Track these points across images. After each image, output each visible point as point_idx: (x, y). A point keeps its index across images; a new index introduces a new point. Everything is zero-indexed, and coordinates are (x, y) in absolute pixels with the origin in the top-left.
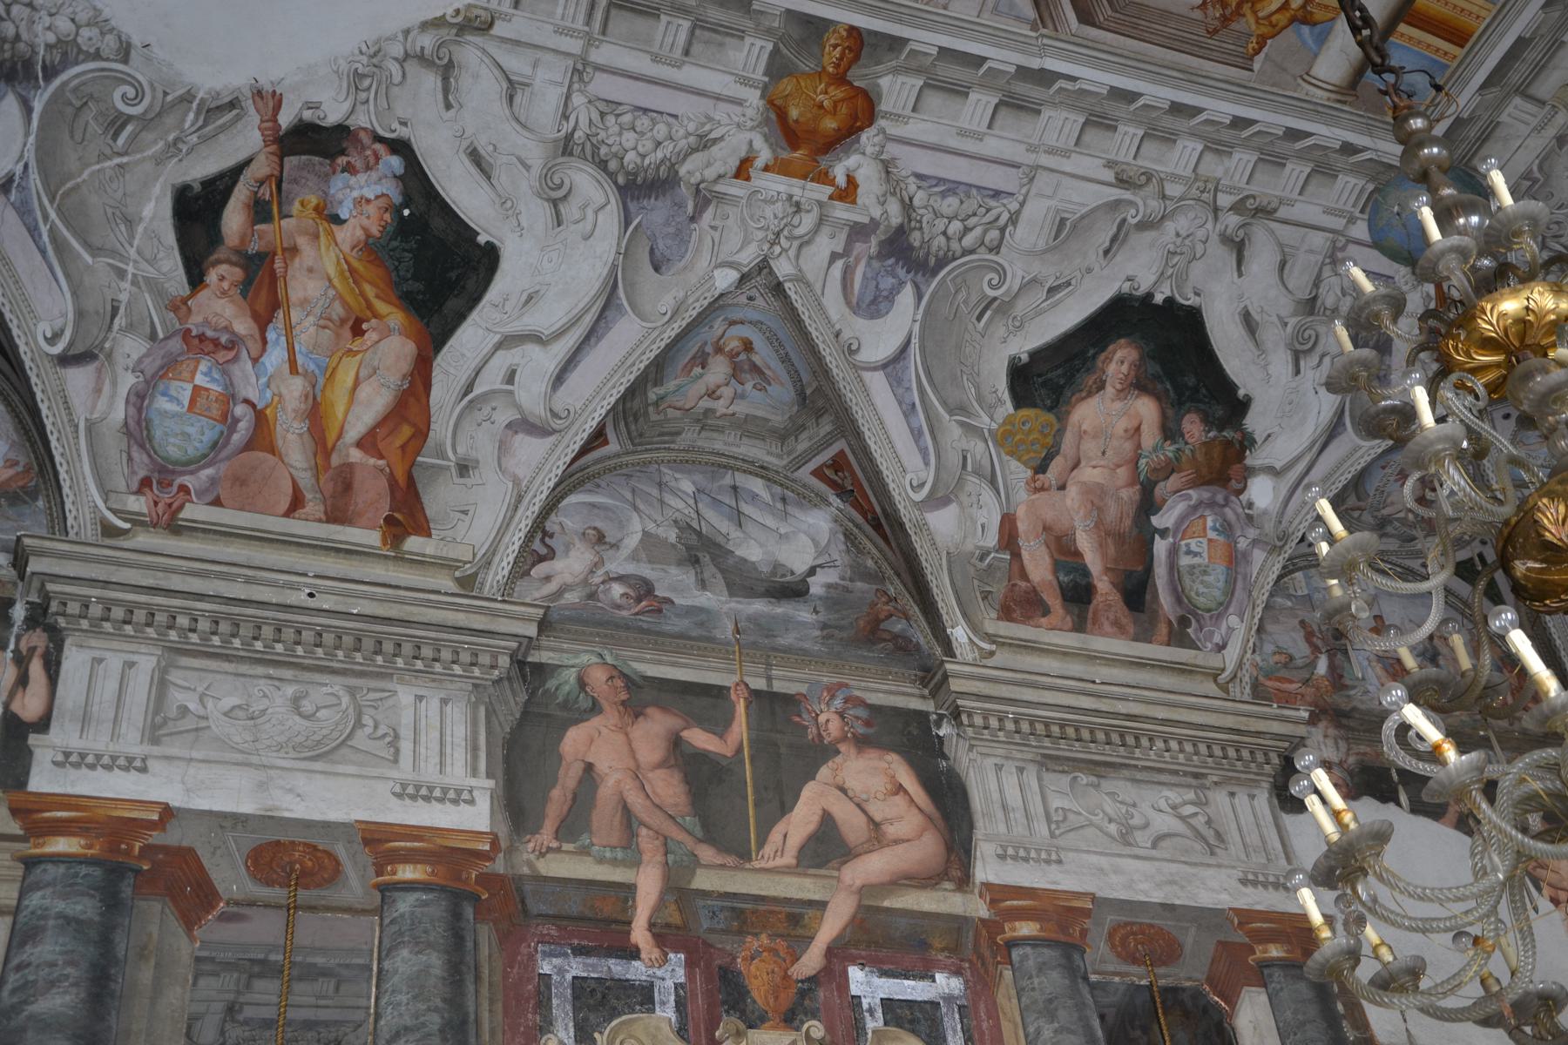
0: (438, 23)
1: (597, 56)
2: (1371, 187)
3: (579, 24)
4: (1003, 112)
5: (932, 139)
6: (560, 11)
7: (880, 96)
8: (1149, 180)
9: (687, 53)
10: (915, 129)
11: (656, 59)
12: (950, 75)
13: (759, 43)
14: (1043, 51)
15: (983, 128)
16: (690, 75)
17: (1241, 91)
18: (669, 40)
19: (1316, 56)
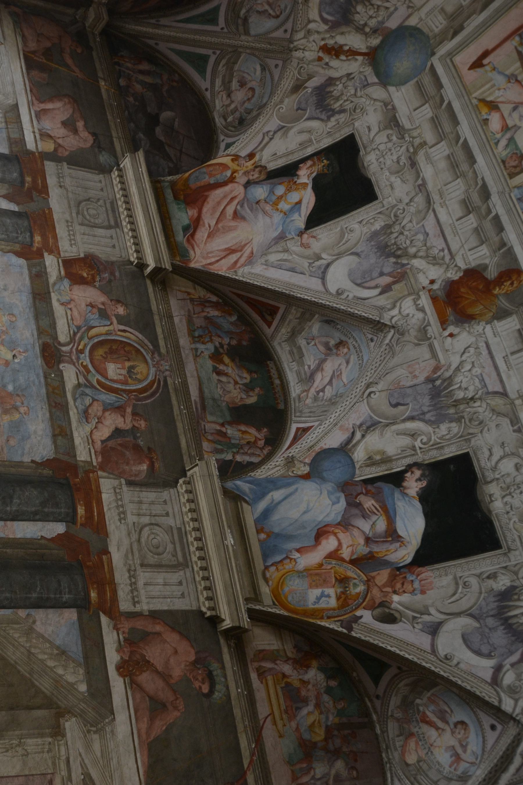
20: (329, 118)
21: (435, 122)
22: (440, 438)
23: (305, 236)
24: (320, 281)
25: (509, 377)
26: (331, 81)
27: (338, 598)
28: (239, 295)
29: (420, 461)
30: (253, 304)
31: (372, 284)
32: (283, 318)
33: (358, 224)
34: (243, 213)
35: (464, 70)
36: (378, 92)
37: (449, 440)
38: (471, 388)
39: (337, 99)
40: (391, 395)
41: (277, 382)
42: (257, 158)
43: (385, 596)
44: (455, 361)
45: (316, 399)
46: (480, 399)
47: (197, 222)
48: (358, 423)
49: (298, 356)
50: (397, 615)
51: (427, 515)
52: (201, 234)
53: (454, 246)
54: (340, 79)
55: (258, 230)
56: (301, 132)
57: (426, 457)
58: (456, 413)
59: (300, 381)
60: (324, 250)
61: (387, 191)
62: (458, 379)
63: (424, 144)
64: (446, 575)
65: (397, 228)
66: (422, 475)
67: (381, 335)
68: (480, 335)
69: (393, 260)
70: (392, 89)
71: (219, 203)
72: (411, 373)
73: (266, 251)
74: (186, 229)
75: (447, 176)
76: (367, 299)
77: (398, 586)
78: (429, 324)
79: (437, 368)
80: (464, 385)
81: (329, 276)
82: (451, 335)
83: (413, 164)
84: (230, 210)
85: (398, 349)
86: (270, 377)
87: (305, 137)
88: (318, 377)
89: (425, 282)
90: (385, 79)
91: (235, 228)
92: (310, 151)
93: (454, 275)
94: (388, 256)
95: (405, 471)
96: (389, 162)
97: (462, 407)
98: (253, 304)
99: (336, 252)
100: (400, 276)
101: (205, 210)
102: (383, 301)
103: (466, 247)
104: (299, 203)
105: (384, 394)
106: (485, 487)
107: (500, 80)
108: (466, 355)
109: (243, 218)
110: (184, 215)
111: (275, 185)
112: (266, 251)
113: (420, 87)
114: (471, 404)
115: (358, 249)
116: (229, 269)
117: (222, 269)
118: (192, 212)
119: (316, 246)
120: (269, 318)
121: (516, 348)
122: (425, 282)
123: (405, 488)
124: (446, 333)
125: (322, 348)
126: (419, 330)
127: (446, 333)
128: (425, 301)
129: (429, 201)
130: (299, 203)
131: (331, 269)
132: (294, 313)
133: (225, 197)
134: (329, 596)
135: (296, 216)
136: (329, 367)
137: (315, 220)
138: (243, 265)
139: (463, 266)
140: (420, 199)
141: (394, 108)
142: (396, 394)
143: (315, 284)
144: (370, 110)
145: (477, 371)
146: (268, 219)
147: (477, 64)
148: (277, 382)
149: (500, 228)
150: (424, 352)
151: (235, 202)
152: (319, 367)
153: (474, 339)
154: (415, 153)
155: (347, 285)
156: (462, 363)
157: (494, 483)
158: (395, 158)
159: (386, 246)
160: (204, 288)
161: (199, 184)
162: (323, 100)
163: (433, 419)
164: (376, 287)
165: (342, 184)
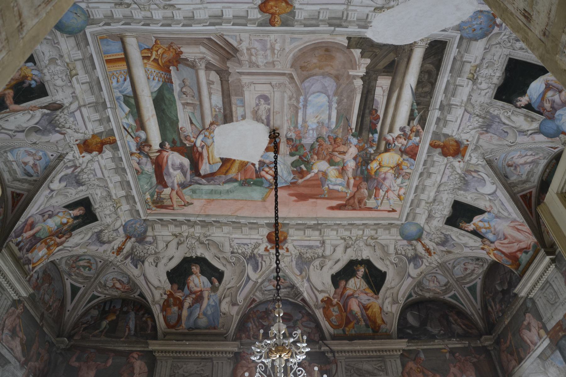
0: (388, 8)
1: (345, 7)
2: (91, 17)
3: (350, 13)
4: (220, 14)
5: (238, 5)
6: (356, 15)
7: (259, 12)
8: (164, 8)
9: (319, 12)
10: (246, 6)
11: (328, 9)
12: (241, 20)
13: (299, 18)
14: (217, 30)
15: (224, 10)
16: (317, 8)
17: (153, 32)
18: (325, 14)
19: (138, 42)
20: (448, 235)
21: (418, 206)
23: (488, 210)
24: (497, 193)
25: (460, 115)
26: (437, 244)
28: (531, 213)
30: (529, 205)
31: (479, 177)
32: (523, 191)
33: (468, 198)
34: (502, 236)
35: (398, 212)
36: (427, 228)
38: (475, 119)
39: (440, 238)
41: (548, 170)
42: (482, 246)
44: (473, 132)
45: (537, 154)
46: (475, 114)
47: (521, 250)
49: (530, 173)
52: (523, 245)
53: (443, 167)
54: (434, 242)
55: (503, 226)
56: (460, 240)
59: (538, 164)
60: (486, 200)
61: (450, 199)
62: (477, 125)
63: (427, 203)
65: (456, 186)
67: (491, 159)
68: (458, 134)
69: (466, 178)
70: (422, 225)
71: (507, 247)
73: (506, 218)
74: (526, 253)
75: (428, 188)
76: (485, 173)
78: (472, 150)
79: (481, 134)
80: (477, 122)
81: (492, 191)
82: (468, 141)
83: (435, 200)
84: (506, 241)
85: (489, 150)
86: (548, 174)
87: (461, 237)
88: (529, 160)
89: (462, 163)
90: (422, 230)
91: (510, 235)
92: (463, 232)
93: (451, 158)
94: (467, 181)
96: (441, 207)
97: (483, 115)
98: (529, 205)
99: (482, 196)
100: (468, 171)
101: (514, 251)
102: (481, 169)
103: (440, 164)
104: (481, 221)
107: (391, 201)
109: (504, 235)
110: (522, 257)
111: (483, 234)
112: (506, 218)
113: (414, 219)
114: (479, 114)
115: (474, 191)
116: (524, 226)
117: (526, 228)
118: (519, 254)
119: (488, 204)
120: (528, 195)
121: (450, 122)
122: (462, 163)
124: (468, 143)
125: (518, 169)
126: (476, 150)
127: (468, 143)
128: (467, 158)
129: (439, 186)
130: (481, 221)
131: (489, 193)
132: (516, 190)
133: (503, 247)
135: (486, 218)
136: (522, 161)
137: (481, 212)
138: (518, 222)
139: (446, 159)
140: (442, 189)
141: (426, 220)
143: (499, 193)
144: (433, 226)
145: (468, 124)
146: (496, 226)
147: (394, 211)
148: (548, 170)
149: (425, 161)
150: (481, 142)
151: (502, 242)
152: (526, 163)
153: (461, 134)
154: (431, 203)
155: (488, 183)
156: (471, 130)
158: (438, 206)
159: (464, 184)
160: (541, 228)
161: (508, 260)
162: (445, 241)
164: (479, 175)
165: (461, 214)
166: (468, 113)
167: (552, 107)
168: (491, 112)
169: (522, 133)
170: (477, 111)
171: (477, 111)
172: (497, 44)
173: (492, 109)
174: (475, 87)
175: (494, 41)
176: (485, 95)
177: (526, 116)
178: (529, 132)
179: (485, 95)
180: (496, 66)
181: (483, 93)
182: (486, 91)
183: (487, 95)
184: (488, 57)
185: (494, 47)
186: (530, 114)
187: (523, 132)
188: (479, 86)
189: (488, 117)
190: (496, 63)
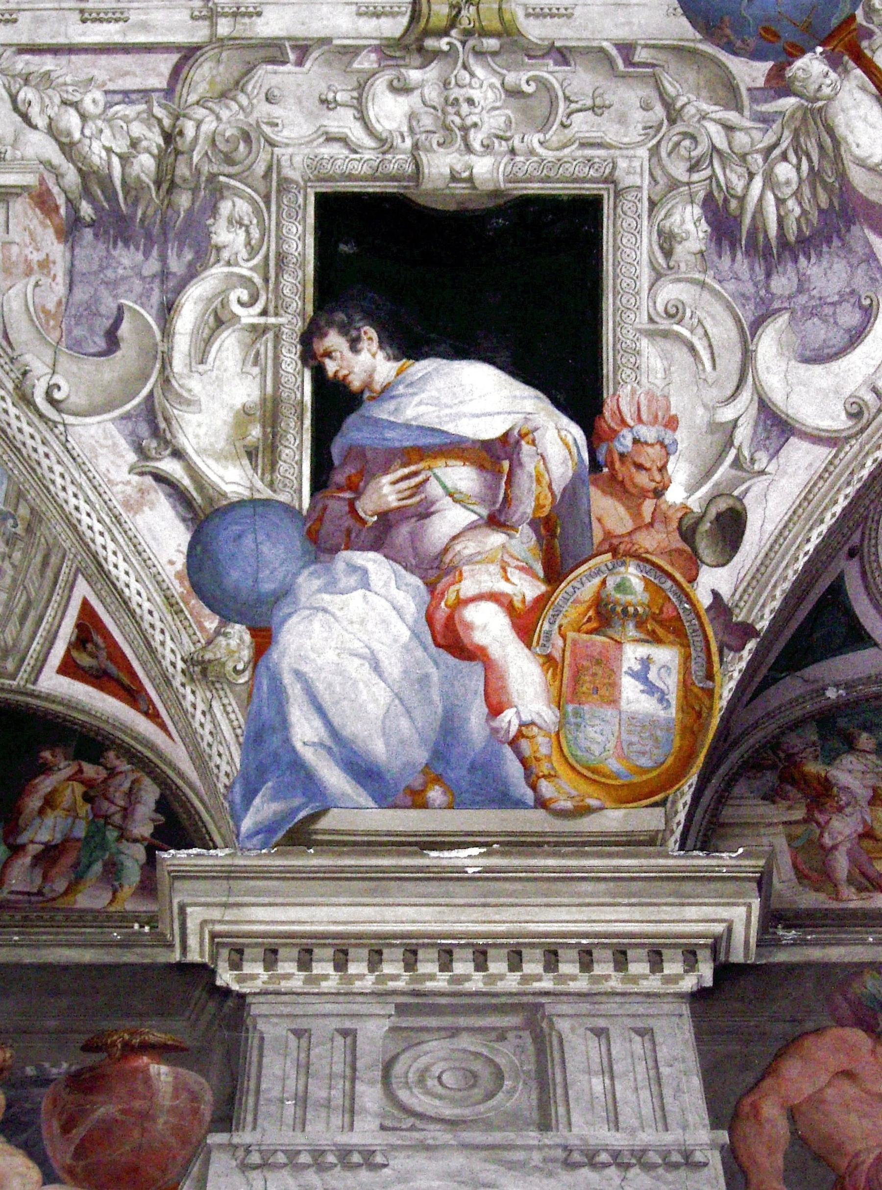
22: (253, 251)
27: (655, 639)
29: (299, 326)
37: (264, 232)
38: (137, 129)
40: (77, 347)
43: (666, 520)
44: (39, 145)
48: (132, 457)
50: (722, 505)
51: (462, 349)
57: (296, 304)
58: (195, 191)
62: (96, 154)
64: (638, 353)
66: (344, 330)
72: (29, 272)
77: (642, 479)
79: (42, 200)
80: (121, 146)
95: (319, 374)
97: (183, 170)
105: (63, 360)
106: (427, 185)
108: (34, 112)
114: (182, 144)
123: (368, 385)
134: (646, 662)
142: (78, 332)
145: (92, 101)
156: (52, 130)
157: (424, 157)
163: (189, 256)
166: (176, 72)
167: (387, 520)
168: (225, 207)
169: (143, 429)
170: (204, 125)
171: (204, 125)
172: (668, 104)
173: (243, 207)
174: (367, 62)
175: (681, 84)
176: (330, 139)
177: (270, 411)
178: (170, 467)
179: (330, 139)
180: (535, 139)
181: (344, 121)
182: (357, 133)
183: (336, 149)
184: (581, 81)
185: (648, 92)
186: (289, 424)
187: (153, 429)
188: (380, 84)
189: (184, 200)
190: (554, 135)
